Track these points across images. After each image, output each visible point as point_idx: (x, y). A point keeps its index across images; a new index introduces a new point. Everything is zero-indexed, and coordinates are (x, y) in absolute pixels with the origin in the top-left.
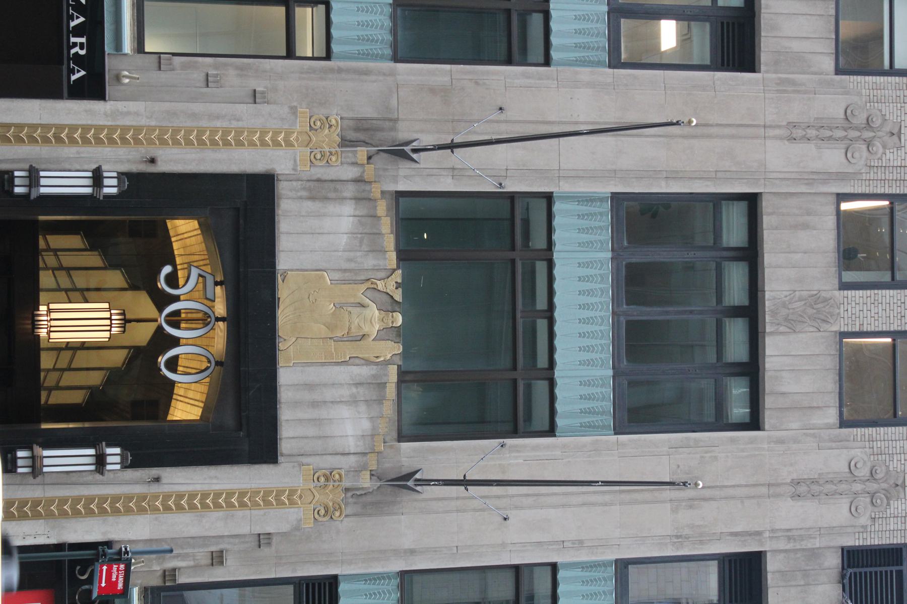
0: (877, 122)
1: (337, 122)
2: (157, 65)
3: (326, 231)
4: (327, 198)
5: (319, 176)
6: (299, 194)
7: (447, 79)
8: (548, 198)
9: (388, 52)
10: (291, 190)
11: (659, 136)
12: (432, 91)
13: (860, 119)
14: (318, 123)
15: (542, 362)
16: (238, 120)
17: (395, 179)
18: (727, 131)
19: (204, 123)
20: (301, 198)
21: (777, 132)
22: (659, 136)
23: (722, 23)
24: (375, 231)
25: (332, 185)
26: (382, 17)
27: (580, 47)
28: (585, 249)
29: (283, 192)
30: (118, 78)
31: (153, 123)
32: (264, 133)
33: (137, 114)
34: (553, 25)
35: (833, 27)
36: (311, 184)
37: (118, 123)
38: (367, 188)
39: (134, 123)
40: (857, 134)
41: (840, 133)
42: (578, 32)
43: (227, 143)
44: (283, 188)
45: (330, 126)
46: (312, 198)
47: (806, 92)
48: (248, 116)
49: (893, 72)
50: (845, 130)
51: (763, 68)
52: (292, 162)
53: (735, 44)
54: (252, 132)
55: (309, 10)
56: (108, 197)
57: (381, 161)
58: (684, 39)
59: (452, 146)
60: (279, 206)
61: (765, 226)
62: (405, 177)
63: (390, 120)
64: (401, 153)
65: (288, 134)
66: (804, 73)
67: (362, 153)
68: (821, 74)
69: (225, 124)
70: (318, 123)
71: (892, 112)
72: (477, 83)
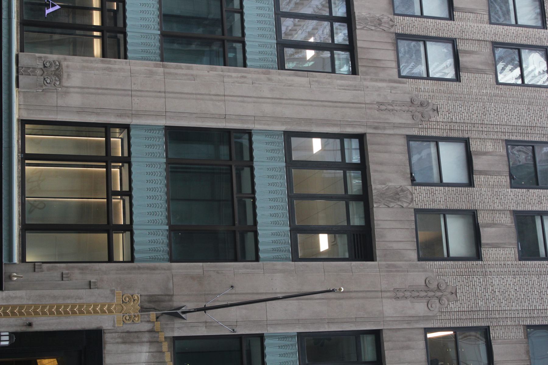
0: (443, 287)
1: (138, 298)
2: (33, 269)
3: (133, 362)
4: (132, 343)
5: (128, 329)
6: (117, 341)
7: (201, 271)
8: (261, 337)
9: (167, 257)
10: (112, 338)
11: (323, 299)
12: (193, 278)
13: (434, 286)
14: (127, 299)
16: (81, 299)
17: (172, 330)
18: (360, 294)
19: (60, 301)
20: (118, 343)
21: (389, 294)
22: (323, 299)
23: (354, 235)
24: (161, 360)
25: (136, 334)
26: (163, 237)
29: (107, 340)
30: (10, 277)
31: (31, 303)
32: (96, 306)
33: (21, 298)
34: (260, 239)
35: (414, 235)
36: (124, 334)
37: (10, 303)
38: (156, 335)
39: (20, 303)
40: (432, 294)
41: (423, 294)
42: (274, 242)
43: (74, 313)
44: (107, 337)
45: (134, 300)
46: (124, 343)
47: (402, 271)
48: (86, 296)
49: (449, 258)
50: (426, 292)
51: (378, 258)
52: (112, 322)
53: (361, 244)
54: (89, 305)
55: (121, 235)
56: (4, 347)
57: (164, 319)
58: (332, 244)
59: (205, 309)
60: (105, 347)
61: (385, 348)
62: (178, 328)
63: (169, 295)
64: (176, 314)
65: (110, 306)
66: (401, 261)
67: (153, 315)
68: (410, 261)
69: (73, 301)
70: (127, 299)
71: (451, 281)
72: (218, 273)
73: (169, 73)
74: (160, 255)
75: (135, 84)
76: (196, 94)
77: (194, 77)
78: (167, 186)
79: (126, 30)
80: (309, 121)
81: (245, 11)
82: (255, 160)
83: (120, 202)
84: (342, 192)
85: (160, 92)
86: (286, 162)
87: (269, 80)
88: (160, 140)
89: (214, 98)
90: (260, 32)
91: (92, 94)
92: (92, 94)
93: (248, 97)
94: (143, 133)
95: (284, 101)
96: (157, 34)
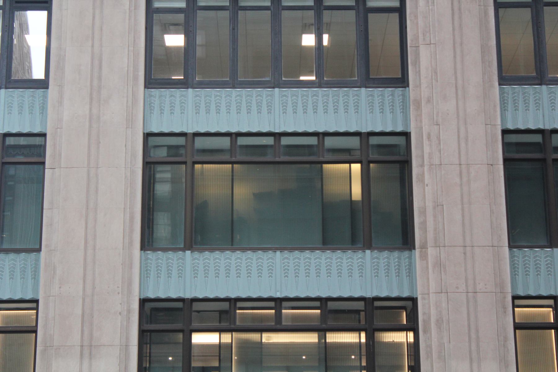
15: (538, 138)
27: (393, 109)
28: (541, 106)
34: (378, 129)
73: (436, 240)
74: (405, 262)
75: (457, 288)
76: (462, 204)
77: (437, 206)
78: (212, 250)
79: (369, 298)
80: (484, 49)
81: (321, 130)
82: (541, 127)
83: (549, 313)
84: (226, 14)
85: (465, 254)
86: (274, 88)
87: (429, 101)
88: (156, 258)
89: (465, 179)
90: (352, 109)
91: (478, 346)
92: (478, 346)
93: (458, 132)
94: (520, 278)
95: (460, 82)
96: (372, 256)
